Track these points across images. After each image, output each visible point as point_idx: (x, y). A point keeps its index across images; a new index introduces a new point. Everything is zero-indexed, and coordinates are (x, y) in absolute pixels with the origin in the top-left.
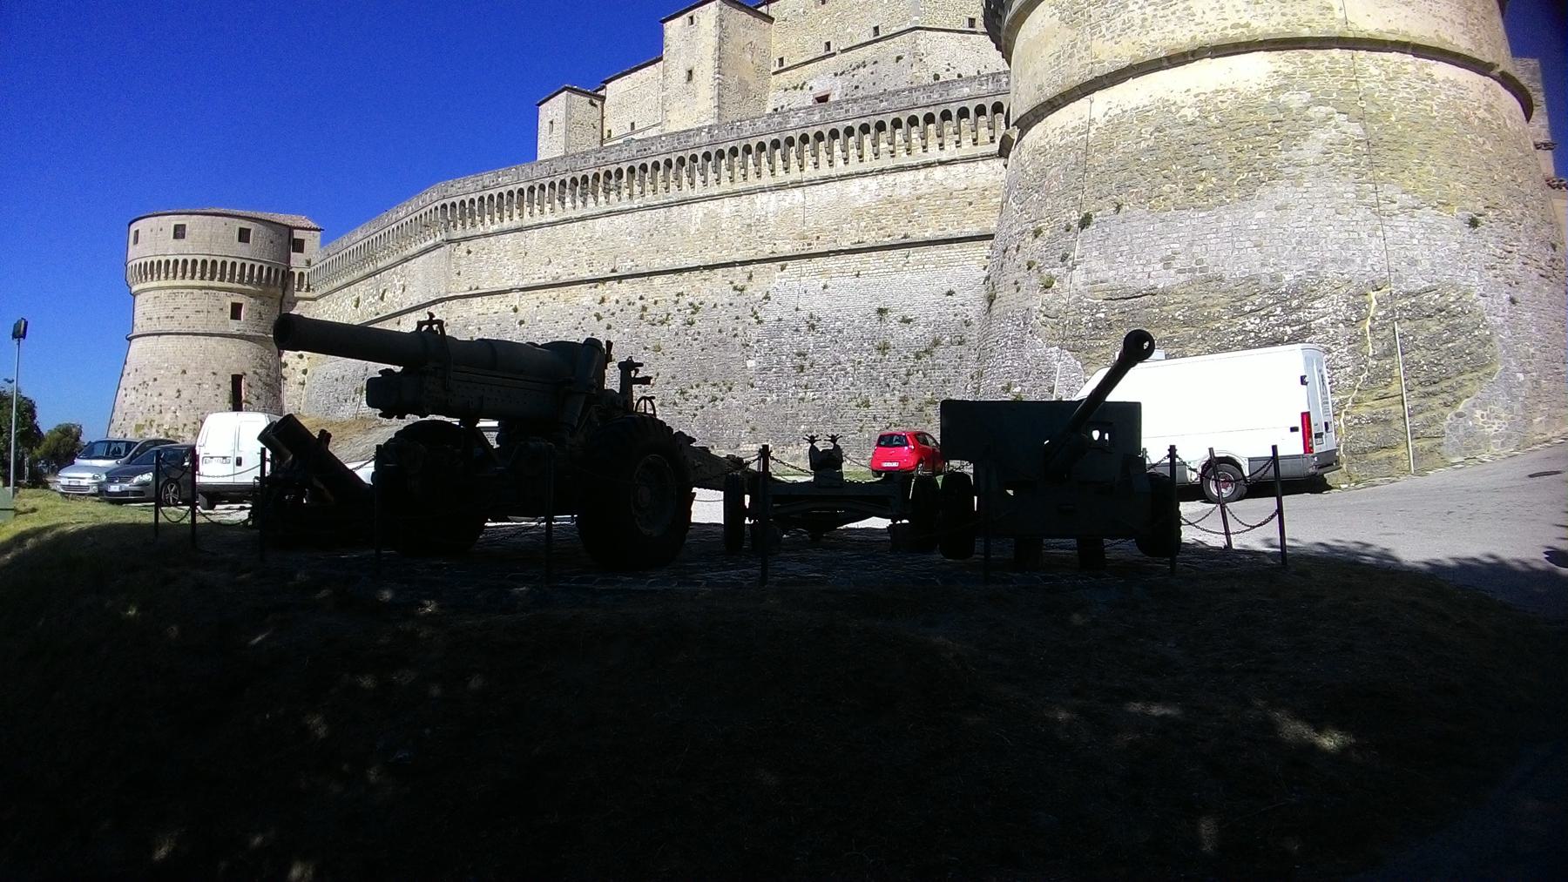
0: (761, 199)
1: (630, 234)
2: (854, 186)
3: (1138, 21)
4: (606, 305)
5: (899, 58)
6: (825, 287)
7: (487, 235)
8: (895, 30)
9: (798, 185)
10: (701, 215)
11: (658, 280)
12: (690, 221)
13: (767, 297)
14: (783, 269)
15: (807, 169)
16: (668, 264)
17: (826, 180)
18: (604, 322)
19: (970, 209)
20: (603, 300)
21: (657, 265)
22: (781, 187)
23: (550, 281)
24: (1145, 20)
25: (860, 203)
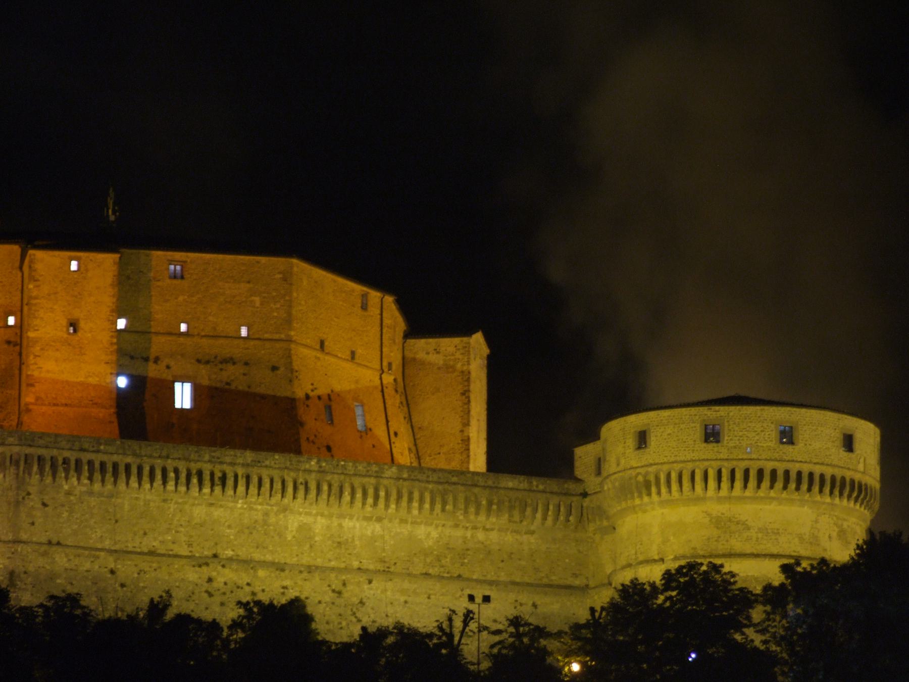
0: (347, 523)
1: (229, 527)
2: (421, 531)
3: (754, 539)
4: (215, 585)
5: (274, 368)
6: (406, 602)
7: (69, 493)
8: (267, 336)
9: (379, 519)
10: (296, 524)
11: (261, 573)
12: (286, 528)
13: (362, 603)
14: (370, 582)
15: (390, 511)
16: (269, 558)
17: (403, 521)
18: (217, 599)
19: (501, 565)
20: (210, 580)
21: (257, 556)
22: (368, 519)
23: (146, 550)
24: (757, 538)
25: (426, 545)
